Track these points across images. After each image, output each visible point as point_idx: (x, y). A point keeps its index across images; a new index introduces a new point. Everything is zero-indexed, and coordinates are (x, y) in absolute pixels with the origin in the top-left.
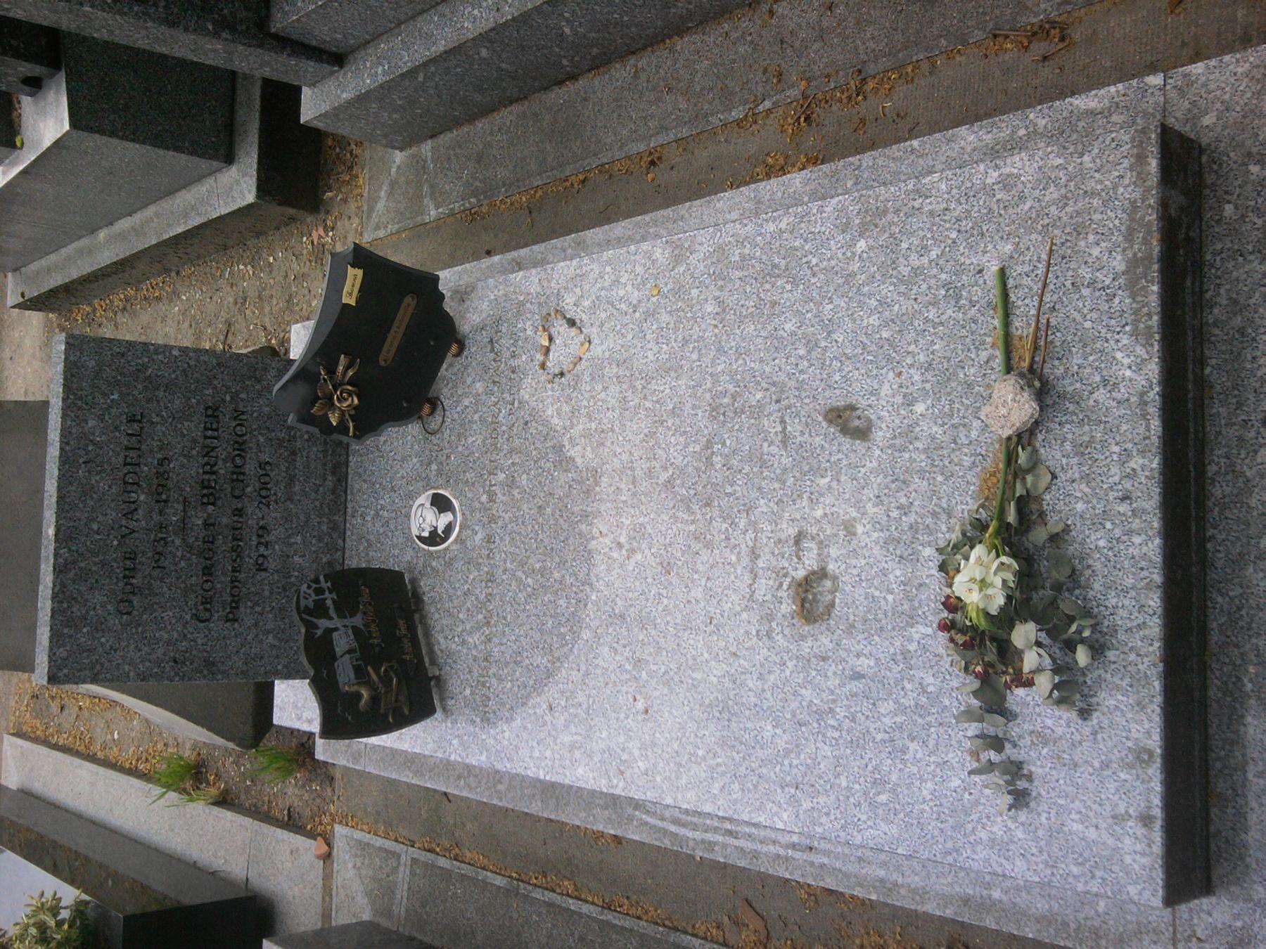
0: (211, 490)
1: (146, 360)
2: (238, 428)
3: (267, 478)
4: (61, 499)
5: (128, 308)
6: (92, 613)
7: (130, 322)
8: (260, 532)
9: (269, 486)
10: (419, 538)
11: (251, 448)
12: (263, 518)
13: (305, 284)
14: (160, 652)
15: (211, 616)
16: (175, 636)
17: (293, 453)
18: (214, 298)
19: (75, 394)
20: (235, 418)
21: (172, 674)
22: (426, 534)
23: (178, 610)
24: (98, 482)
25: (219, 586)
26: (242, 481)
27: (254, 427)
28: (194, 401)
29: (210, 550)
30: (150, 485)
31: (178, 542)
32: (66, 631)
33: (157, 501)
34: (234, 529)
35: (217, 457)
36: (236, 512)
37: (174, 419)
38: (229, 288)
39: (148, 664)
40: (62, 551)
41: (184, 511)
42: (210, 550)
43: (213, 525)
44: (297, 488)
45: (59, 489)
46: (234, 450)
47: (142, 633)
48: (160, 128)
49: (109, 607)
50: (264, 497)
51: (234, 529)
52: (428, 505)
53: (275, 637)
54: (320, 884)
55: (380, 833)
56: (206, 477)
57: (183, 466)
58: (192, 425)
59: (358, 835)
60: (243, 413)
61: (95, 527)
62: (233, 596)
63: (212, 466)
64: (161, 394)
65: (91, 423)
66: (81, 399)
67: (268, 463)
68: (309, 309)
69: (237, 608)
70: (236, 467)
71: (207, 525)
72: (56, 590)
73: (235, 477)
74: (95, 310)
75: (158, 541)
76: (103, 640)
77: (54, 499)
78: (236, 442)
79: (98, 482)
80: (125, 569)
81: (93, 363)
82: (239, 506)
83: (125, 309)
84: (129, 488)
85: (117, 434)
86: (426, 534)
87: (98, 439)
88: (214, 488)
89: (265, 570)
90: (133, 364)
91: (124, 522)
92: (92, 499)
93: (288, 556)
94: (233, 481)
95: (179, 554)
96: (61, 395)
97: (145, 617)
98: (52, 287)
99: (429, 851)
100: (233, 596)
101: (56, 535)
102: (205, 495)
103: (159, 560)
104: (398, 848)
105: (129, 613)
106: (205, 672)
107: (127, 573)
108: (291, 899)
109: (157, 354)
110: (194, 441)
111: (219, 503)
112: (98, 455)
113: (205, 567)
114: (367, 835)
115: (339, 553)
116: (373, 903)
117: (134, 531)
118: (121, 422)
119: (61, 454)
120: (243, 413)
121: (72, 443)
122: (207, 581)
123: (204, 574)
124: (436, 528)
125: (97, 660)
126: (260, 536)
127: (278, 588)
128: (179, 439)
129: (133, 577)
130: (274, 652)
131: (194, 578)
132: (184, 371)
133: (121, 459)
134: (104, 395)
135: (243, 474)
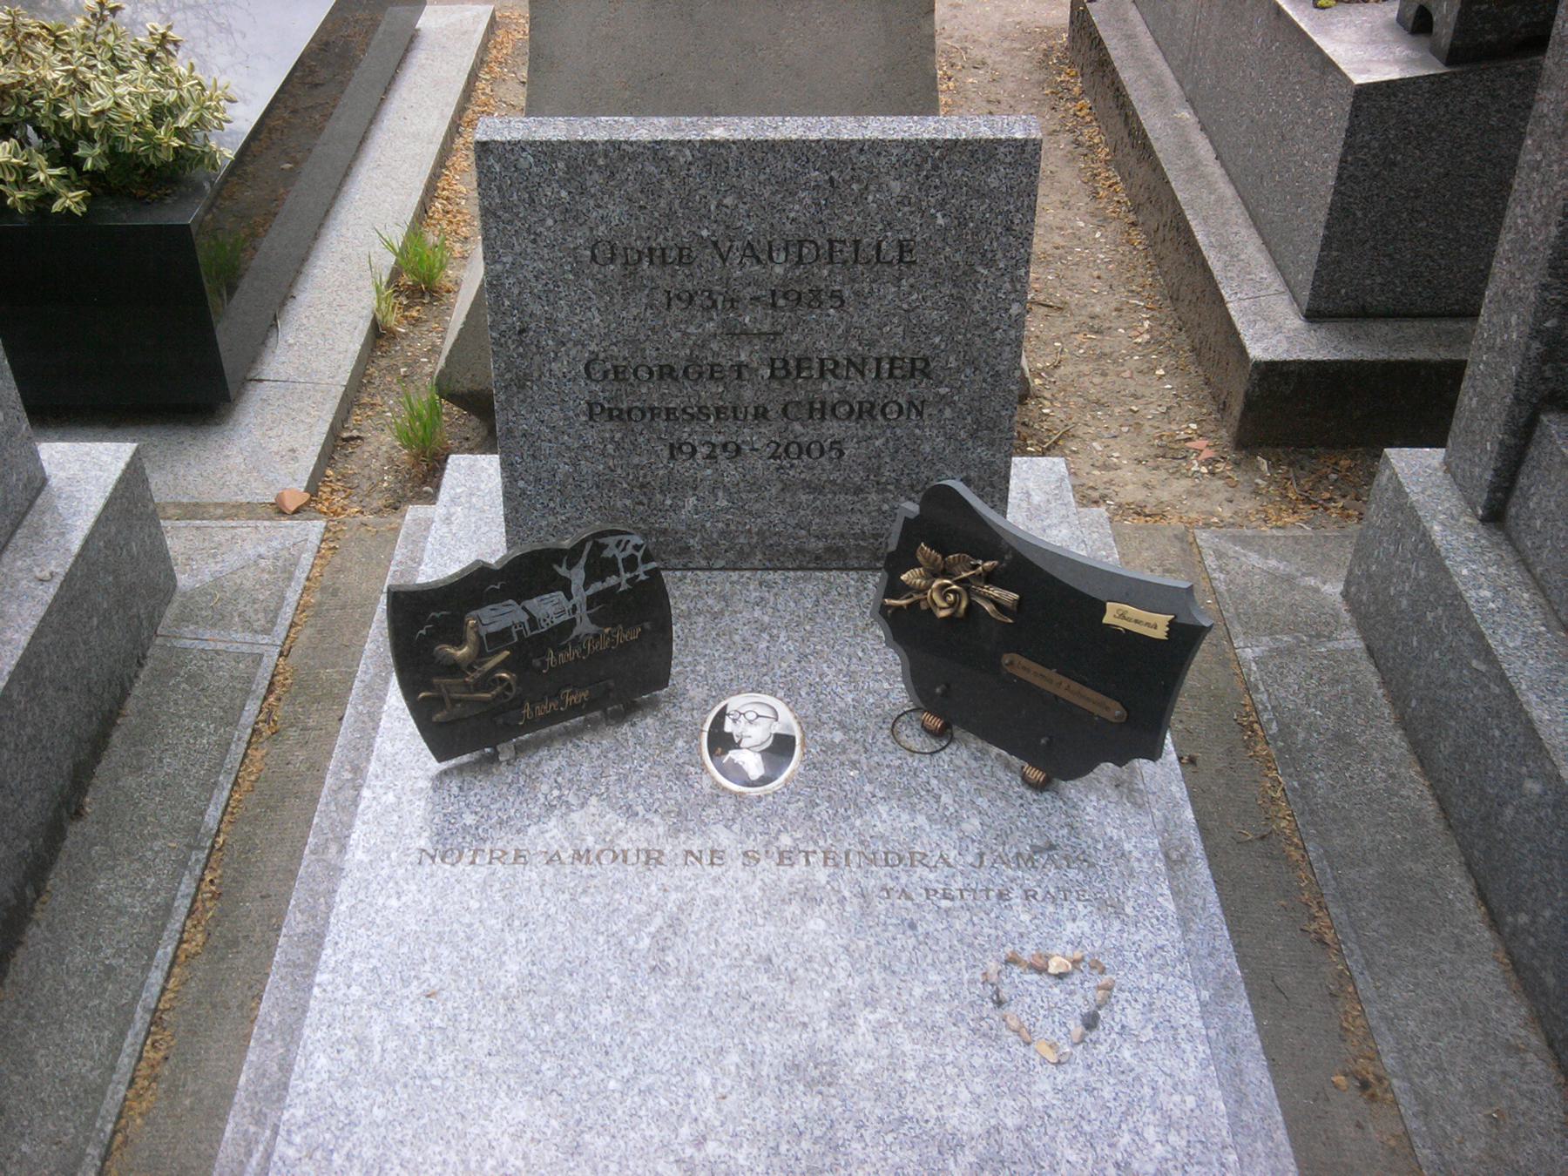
0: (795, 373)
1: (1002, 265)
2: (896, 408)
3: (816, 454)
4: (772, 146)
5: (1081, 150)
6: (592, 203)
7: (1060, 153)
8: (731, 447)
9: (805, 457)
10: (722, 714)
11: (864, 428)
12: (753, 449)
13: (1125, 429)
14: (537, 308)
15: (598, 381)
16: (562, 330)
17: (858, 490)
18: (1098, 283)
19: (941, 159)
20: (911, 403)
21: (503, 327)
22: (729, 726)
23: (602, 331)
25: (644, 390)
26: (811, 417)
27: (898, 431)
28: (937, 340)
29: (700, 374)
30: (799, 281)
31: (710, 326)
32: (561, 165)
33: (773, 293)
34: (735, 409)
35: (848, 378)
36: (761, 410)
37: (907, 311)
38: (1114, 305)
39: (516, 291)
40: (688, 152)
41: (760, 334)
42: (700, 374)
43: (740, 376)
44: (804, 498)
45: (787, 143)
46: (861, 403)
47: (566, 281)
48: (1359, 214)
49: (602, 228)
50: (786, 450)
51: (735, 409)
52: (778, 728)
53: (567, 475)
54: (242, 499)
55: (306, 598)
56: (816, 365)
57: (832, 328)
58: (897, 339)
59: (307, 559)
60: (920, 414)
61: (728, 201)
62: (629, 411)
63: (833, 372)
64: (947, 289)
65: (896, 186)
66: (935, 168)
67: (842, 453)
68: (1087, 437)
69: (611, 418)
70: (833, 409)
71: (739, 368)
72: (624, 146)
73: (818, 406)
74: (1076, 100)
75: (709, 297)
76: (550, 222)
77: (771, 135)
78: (873, 405)
79: (800, 201)
80: (663, 250)
81: (996, 184)
82: (771, 414)
83: (1078, 144)
84: (792, 249)
85: (880, 226)
86: (729, 726)
87: (870, 198)
88: (798, 376)
89: (672, 456)
90: (995, 244)
91: (737, 244)
92: (773, 194)
93: (695, 489)
94: (811, 404)
95: (692, 329)
96: (940, 137)
97: (590, 283)
98: (1106, 42)
99: (271, 684)
100: (629, 411)
101: (713, 142)
102: (786, 362)
103: (680, 299)
104: (281, 629)
105: (594, 258)
106: (508, 376)
107: (658, 253)
108: (227, 452)
109: (1012, 281)
110: (872, 344)
111: (775, 385)
112: (844, 200)
113: (672, 369)
114: (305, 575)
115: (704, 563)
116: (203, 591)
117: (724, 261)
118: (898, 231)
119: (845, 142)
120: (920, 414)
121: (862, 158)
122: (651, 373)
123: (661, 367)
124: (737, 746)
125: (517, 215)
126: (725, 446)
127: (645, 476)
128: (875, 320)
129: (651, 262)
130: (544, 475)
131: (655, 354)
132: (985, 323)
133: (838, 234)
134: (942, 204)
135: (823, 418)
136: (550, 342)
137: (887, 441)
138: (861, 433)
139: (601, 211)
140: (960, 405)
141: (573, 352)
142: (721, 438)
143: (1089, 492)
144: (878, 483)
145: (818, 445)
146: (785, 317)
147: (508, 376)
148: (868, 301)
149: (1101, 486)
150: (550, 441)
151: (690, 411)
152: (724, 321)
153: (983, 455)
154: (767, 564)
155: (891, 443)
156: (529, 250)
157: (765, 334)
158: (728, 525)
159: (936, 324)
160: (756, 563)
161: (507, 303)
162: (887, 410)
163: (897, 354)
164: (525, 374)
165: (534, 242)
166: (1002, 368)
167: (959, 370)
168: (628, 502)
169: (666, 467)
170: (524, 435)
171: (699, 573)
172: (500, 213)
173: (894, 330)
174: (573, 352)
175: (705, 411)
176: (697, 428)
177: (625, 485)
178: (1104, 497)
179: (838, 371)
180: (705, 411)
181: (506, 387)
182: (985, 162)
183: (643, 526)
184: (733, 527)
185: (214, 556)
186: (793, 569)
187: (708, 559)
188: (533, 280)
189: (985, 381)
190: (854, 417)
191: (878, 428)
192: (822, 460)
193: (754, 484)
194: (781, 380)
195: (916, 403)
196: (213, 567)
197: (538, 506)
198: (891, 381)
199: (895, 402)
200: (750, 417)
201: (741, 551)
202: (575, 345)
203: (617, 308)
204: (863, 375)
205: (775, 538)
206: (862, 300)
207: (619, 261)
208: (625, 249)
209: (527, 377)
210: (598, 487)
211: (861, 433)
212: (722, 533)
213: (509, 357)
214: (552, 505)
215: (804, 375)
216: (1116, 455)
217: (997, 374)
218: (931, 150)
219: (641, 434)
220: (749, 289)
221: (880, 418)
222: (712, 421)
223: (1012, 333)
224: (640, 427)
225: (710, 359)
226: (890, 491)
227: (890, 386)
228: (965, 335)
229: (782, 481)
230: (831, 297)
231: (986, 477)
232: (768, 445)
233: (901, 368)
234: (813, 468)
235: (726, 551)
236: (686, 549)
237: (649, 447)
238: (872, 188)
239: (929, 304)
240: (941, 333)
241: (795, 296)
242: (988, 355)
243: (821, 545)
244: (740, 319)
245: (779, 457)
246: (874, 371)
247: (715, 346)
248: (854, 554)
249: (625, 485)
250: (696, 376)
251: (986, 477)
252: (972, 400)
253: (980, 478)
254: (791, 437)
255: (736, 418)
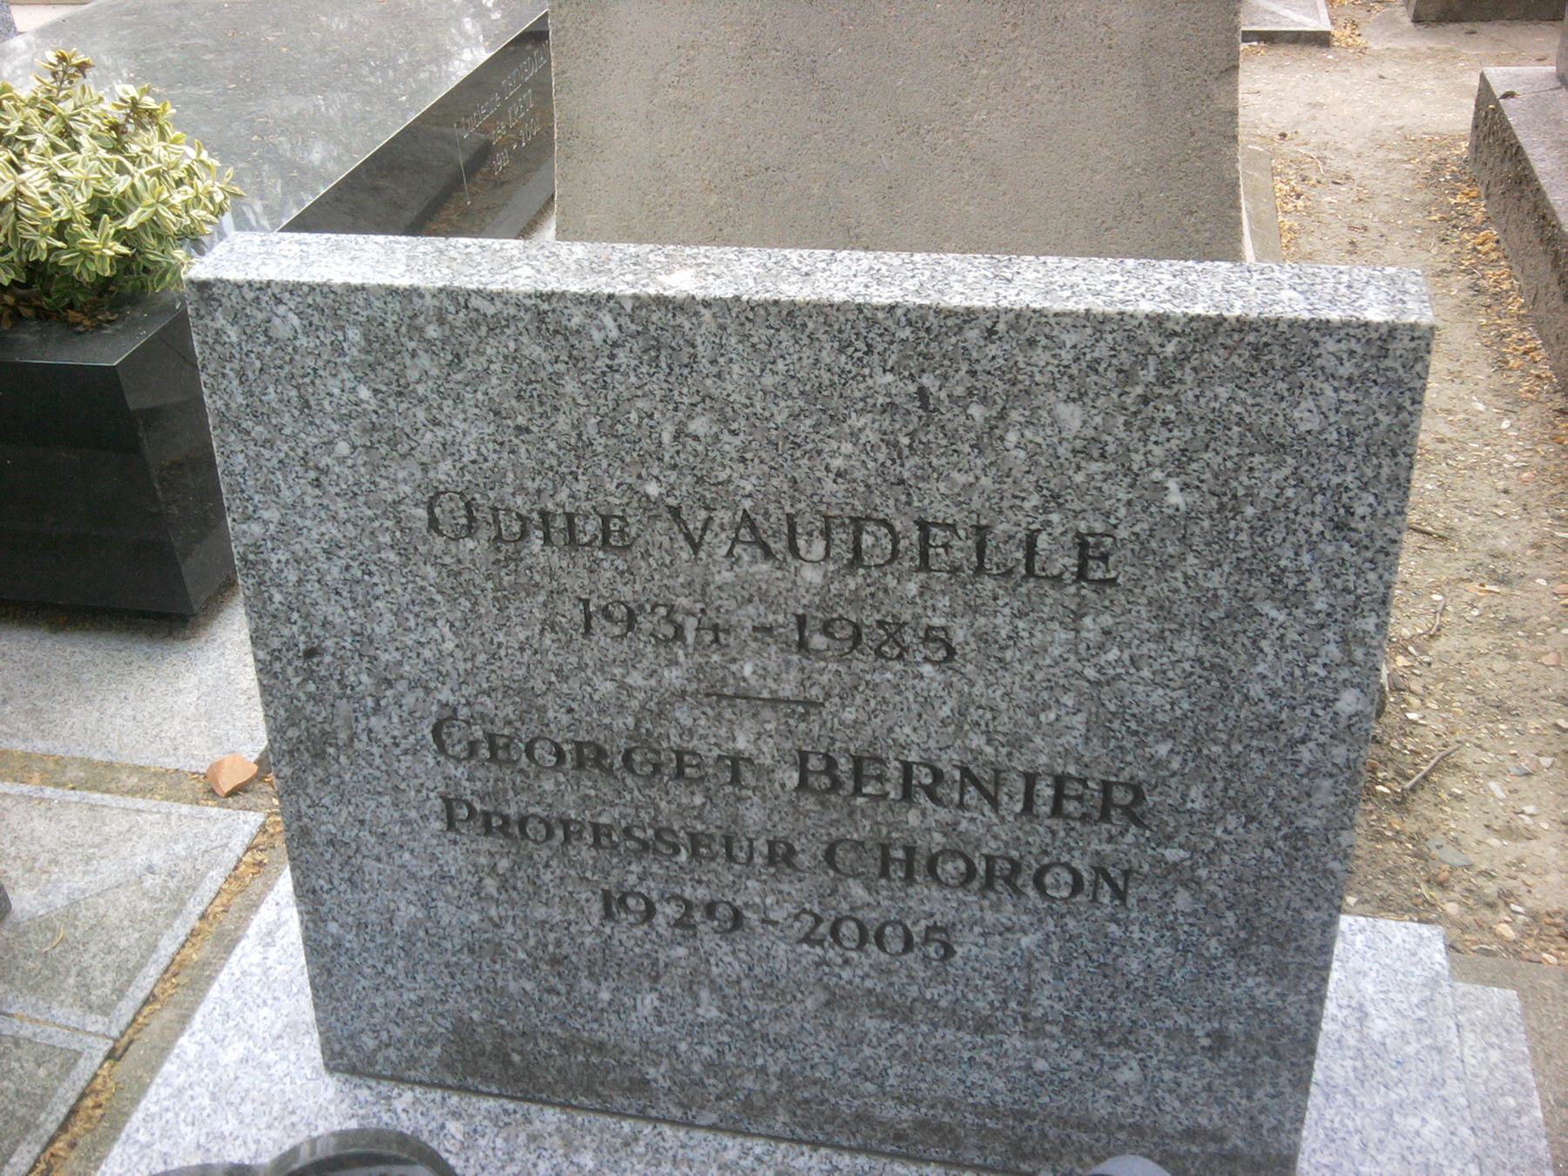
0: (850, 785)
1: (1320, 605)
2: (1066, 877)
3: (897, 946)
5: (1481, 299)
6: (421, 415)
7: (1449, 302)
8: (722, 911)
9: (872, 948)
11: (996, 908)
12: (766, 921)
13: (1546, 761)
14: (331, 610)
15: (458, 760)
16: (384, 657)
17: (983, 1026)
18: (1504, 500)
19: (1181, 359)
20: (1100, 871)
21: (276, 643)
23: (462, 666)
24: (854, 435)
25: (548, 785)
26: (884, 873)
27: (1071, 923)
29: (657, 768)
30: (855, 600)
31: (673, 677)
32: (354, 334)
33: (802, 622)
34: (728, 843)
35: (962, 806)
36: (781, 849)
37: (1098, 683)
38: (1529, 537)
39: (293, 577)
40: (608, 320)
41: (775, 702)
42: (657, 768)
43: (736, 779)
44: (871, 1024)
45: (823, 310)
46: (990, 859)
47: (383, 565)
49: (446, 466)
50: (834, 931)
51: (728, 843)
53: (415, 923)
54: (171, 763)
55: (187, 951)
56: (894, 771)
57: (927, 702)
58: (1073, 739)
59: (215, 878)
60: (1120, 895)
61: (699, 426)
62: (523, 821)
63: (930, 792)
64: (1188, 645)
65: (1071, 416)
66: (1165, 379)
67: (949, 951)
68: (1480, 771)
69: (488, 830)
70: (931, 867)
71: (735, 764)
72: (475, 302)
73: (899, 854)
74: (1476, 229)
75: (669, 618)
76: (343, 448)
78: (1016, 867)
80: (570, 517)
82: (803, 859)
83: (1479, 291)
84: (839, 535)
85: (1035, 500)
87: (1012, 437)
88: (857, 791)
89: (608, 915)
90: (1306, 558)
91: (721, 516)
92: (795, 416)
93: (656, 979)
94: (885, 848)
95: (635, 679)
97: (431, 572)
98: (1528, 151)
99: (73, 1111)
100: (523, 821)
101: (661, 301)
102: (831, 763)
103: (608, 616)
104: (126, 1009)
105: (433, 523)
106: (292, 733)
107: (560, 523)
108: (181, 685)
109: (1344, 641)
110: (1017, 742)
111: (809, 803)
112: (952, 437)
113: (600, 752)
114: (200, 909)
115: (677, 1113)
116: (45, 925)
117: (696, 547)
119: (951, 313)
120: (1120, 895)
121: (993, 350)
122: (560, 755)
123: (579, 746)
125: (280, 429)
126: (710, 909)
127: (558, 943)
128: (1023, 696)
129: (547, 539)
130: (373, 917)
131: (565, 719)
132: (1276, 725)
133: (940, 511)
134: (1181, 460)
135: (909, 878)
136: (364, 678)
137: (1047, 940)
138: (990, 917)
139: (440, 432)
140: (1212, 888)
141: (409, 700)
142: (702, 893)
143: (1481, 881)
144: (1026, 1018)
145: (900, 930)
146: (827, 673)
147: (292, 733)
148: (1008, 655)
149: (1501, 871)
150: (379, 860)
151: (638, 833)
152: (700, 668)
153: (1257, 992)
154: (799, 1131)
155: (1055, 946)
156: (309, 501)
157: (788, 701)
158: (720, 1053)
159: (1160, 717)
160: (778, 1127)
161: (278, 597)
162: (1048, 879)
163: (1072, 770)
164: (324, 733)
165: (317, 483)
166: (1312, 823)
167: (1209, 816)
168: (529, 986)
169: (599, 933)
170: (331, 843)
171: (667, 1131)
172: (247, 424)
173: (1066, 720)
174: (409, 700)
175: (668, 838)
176: (655, 868)
177: (522, 955)
178: (1506, 896)
179: (940, 791)
180: (668, 838)
181: (291, 752)
183: (559, 1032)
184: (730, 1058)
185: (88, 860)
186: (851, 1150)
187: (685, 1107)
188: (322, 557)
189: (1269, 844)
190: (975, 885)
191: (1027, 911)
192: (909, 957)
193: (771, 985)
194: (822, 796)
195: (1113, 872)
196: (79, 882)
197: (367, 971)
198: (1058, 824)
199: (1067, 866)
200: (758, 860)
201: (747, 1104)
202: (411, 688)
203: (487, 624)
204: (995, 803)
205: (816, 1089)
206: (994, 650)
207: (485, 533)
208: (495, 510)
209: (327, 737)
210: (471, 951)
211: (990, 917)
212: (709, 1065)
213: (292, 698)
214: (390, 971)
215: (868, 790)
216: (1530, 809)
217: (1300, 833)
219: (547, 866)
220: (751, 609)
221: (1031, 892)
222: (683, 857)
223: (1340, 753)
224: (545, 853)
225: (675, 739)
226: (1052, 1037)
227: (1053, 833)
228: (1227, 745)
229: (826, 988)
230: (926, 639)
231: (1262, 1035)
232: (797, 917)
233: (1079, 798)
234: (889, 972)
235: (719, 1098)
236: (641, 1085)
237: (563, 892)
239: (1146, 673)
240: (1170, 736)
241: (849, 631)
242: (1280, 794)
243: (906, 1113)
244: (734, 667)
245: (820, 943)
246: (1020, 796)
247: (683, 715)
248: (973, 1140)
249: (522, 955)
250: (648, 769)
251: (1262, 1035)
252: (1239, 880)
253: (1250, 1037)
254: (845, 906)
255: (731, 857)
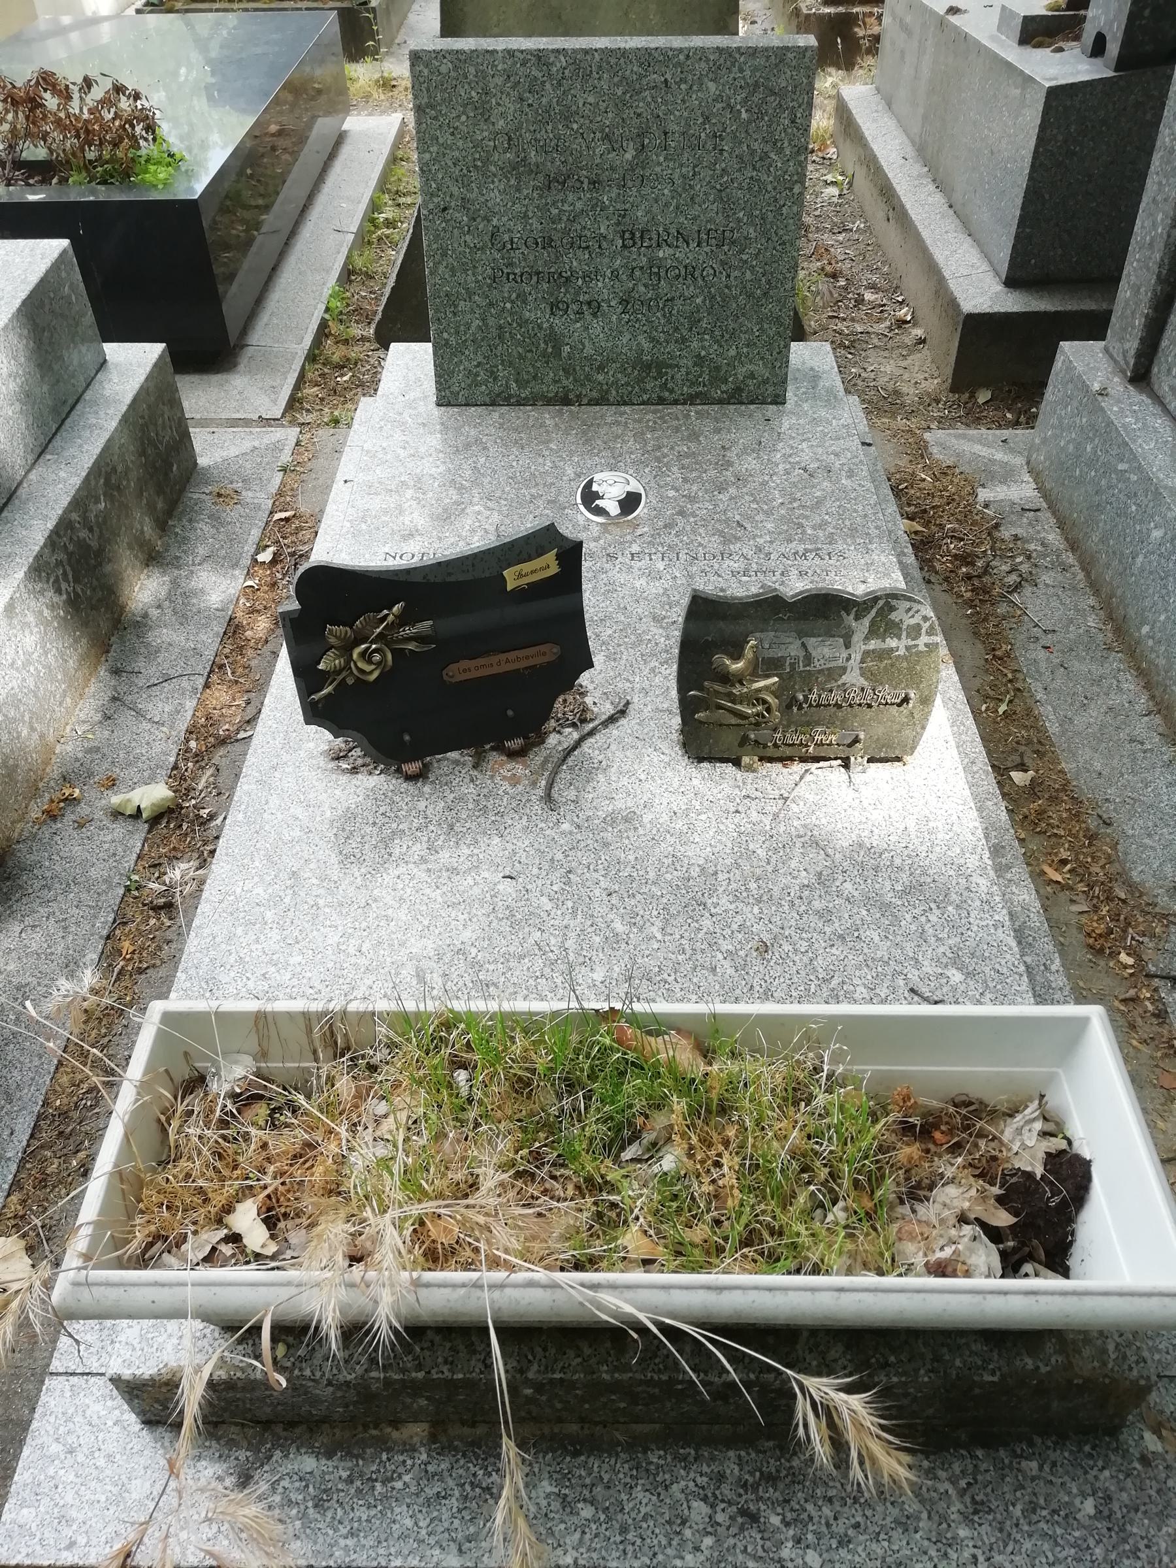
10: (590, 483)
22: (595, 488)
24: (644, 99)
28: (741, 214)
35: (677, 247)
47: (475, 166)
48: (1047, 197)
52: (629, 489)
76: (464, 118)
81: (784, 84)
85: (701, 120)
86: (595, 488)
87: (694, 96)
102: (633, 234)
124: (602, 498)
126: (589, 303)
131: (540, 227)
165: (453, 134)
169: (548, 321)
182: (776, 65)
189: (774, 248)
218: (737, 56)
223: (795, 208)
238: (695, 88)
